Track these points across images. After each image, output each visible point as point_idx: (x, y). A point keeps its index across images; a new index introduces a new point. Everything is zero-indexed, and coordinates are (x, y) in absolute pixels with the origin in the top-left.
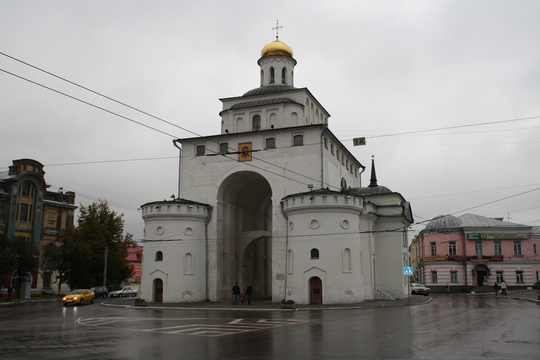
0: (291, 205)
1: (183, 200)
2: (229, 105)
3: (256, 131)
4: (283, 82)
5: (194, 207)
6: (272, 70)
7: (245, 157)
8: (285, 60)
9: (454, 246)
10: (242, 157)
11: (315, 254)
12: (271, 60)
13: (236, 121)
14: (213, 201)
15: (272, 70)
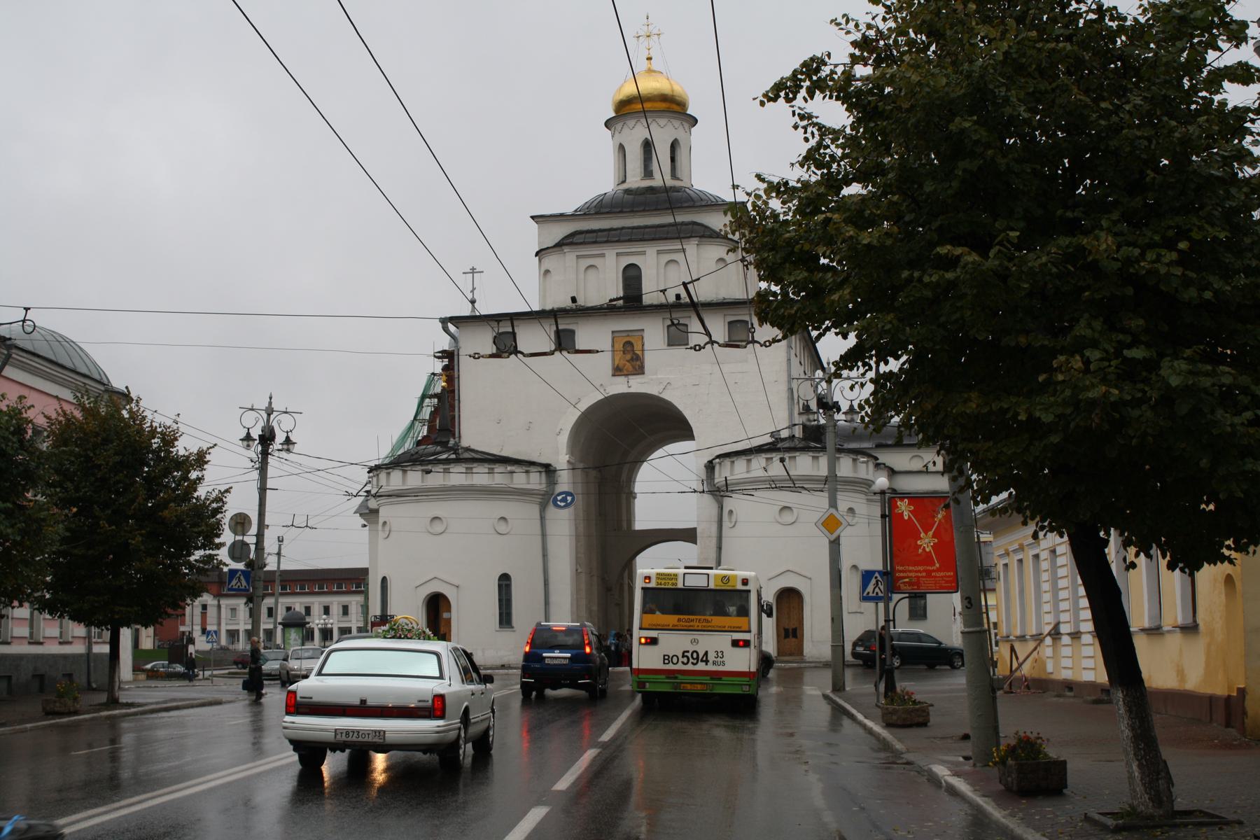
0: (738, 471)
2: (559, 232)
3: (631, 300)
4: (674, 175)
5: (483, 468)
6: (648, 146)
8: (677, 123)
13: (582, 276)
15: (648, 146)
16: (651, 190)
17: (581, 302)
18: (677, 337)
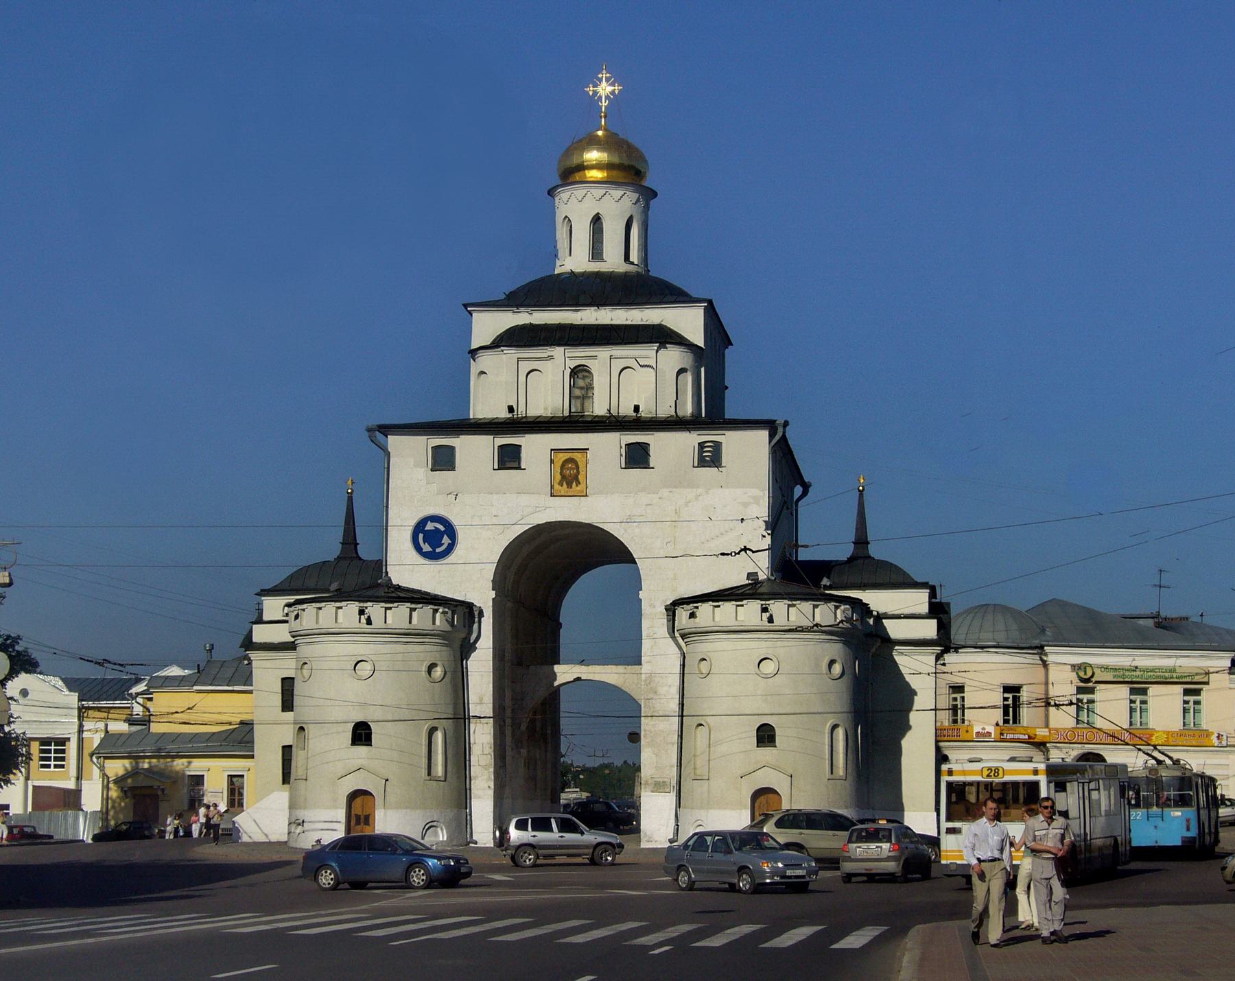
1: (399, 588)
6: (597, 220)
7: (569, 485)
9: (1016, 699)
10: (561, 484)
11: (766, 736)
12: (598, 192)
14: (482, 595)
15: (597, 220)
16: (598, 275)
17: (521, 411)
18: (637, 457)
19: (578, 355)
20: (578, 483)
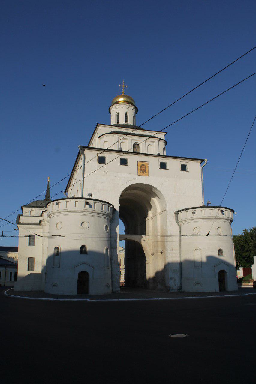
7: (143, 172)
19: (136, 139)
20: (146, 172)
